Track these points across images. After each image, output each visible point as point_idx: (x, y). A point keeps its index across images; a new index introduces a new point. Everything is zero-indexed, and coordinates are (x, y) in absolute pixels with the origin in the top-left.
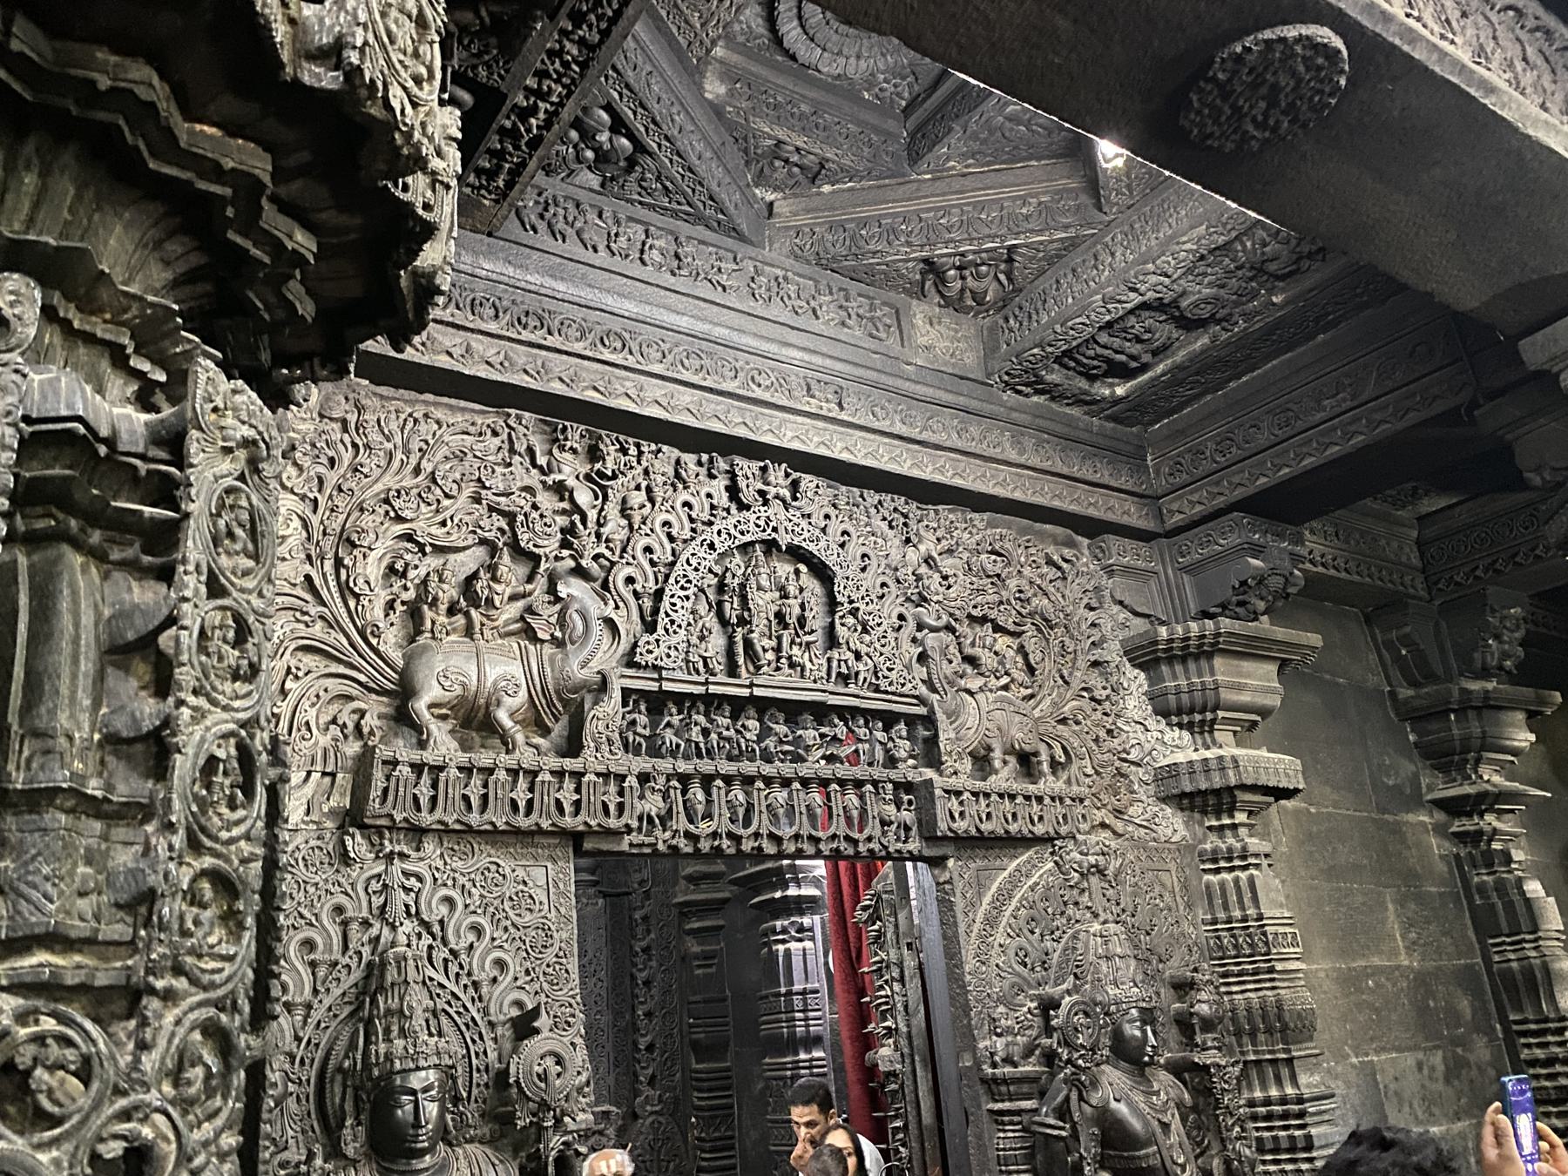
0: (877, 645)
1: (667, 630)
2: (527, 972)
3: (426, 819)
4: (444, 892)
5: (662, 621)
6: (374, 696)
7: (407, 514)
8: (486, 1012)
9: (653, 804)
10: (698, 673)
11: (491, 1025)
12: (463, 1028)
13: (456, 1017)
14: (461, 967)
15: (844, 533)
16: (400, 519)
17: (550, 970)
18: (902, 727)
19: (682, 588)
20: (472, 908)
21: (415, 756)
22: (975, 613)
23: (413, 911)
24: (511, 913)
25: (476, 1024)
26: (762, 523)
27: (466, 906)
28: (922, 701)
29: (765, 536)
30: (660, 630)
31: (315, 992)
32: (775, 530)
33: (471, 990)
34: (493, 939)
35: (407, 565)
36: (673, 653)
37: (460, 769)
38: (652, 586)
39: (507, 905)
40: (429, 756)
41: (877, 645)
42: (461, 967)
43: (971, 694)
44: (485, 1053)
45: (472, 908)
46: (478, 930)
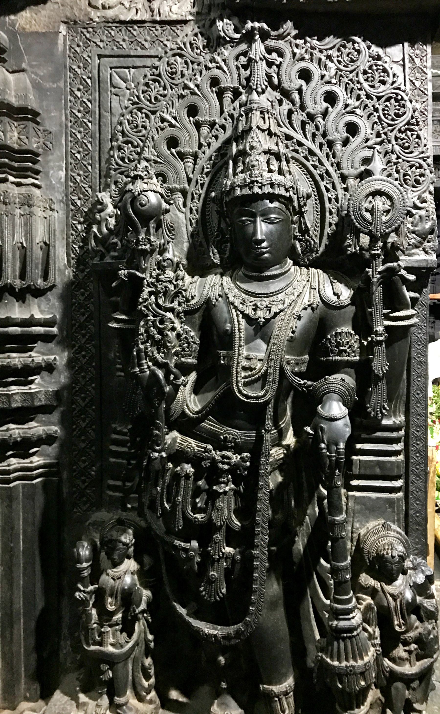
2: (378, 135)
4: (303, 64)
8: (339, 166)
12: (318, 178)
13: (312, 169)
14: (317, 128)
17: (403, 136)
20: (327, 78)
24: (366, 85)
27: (323, 77)
31: (200, 146)
33: (325, 148)
34: (347, 106)
39: (361, 78)
46: (331, 98)
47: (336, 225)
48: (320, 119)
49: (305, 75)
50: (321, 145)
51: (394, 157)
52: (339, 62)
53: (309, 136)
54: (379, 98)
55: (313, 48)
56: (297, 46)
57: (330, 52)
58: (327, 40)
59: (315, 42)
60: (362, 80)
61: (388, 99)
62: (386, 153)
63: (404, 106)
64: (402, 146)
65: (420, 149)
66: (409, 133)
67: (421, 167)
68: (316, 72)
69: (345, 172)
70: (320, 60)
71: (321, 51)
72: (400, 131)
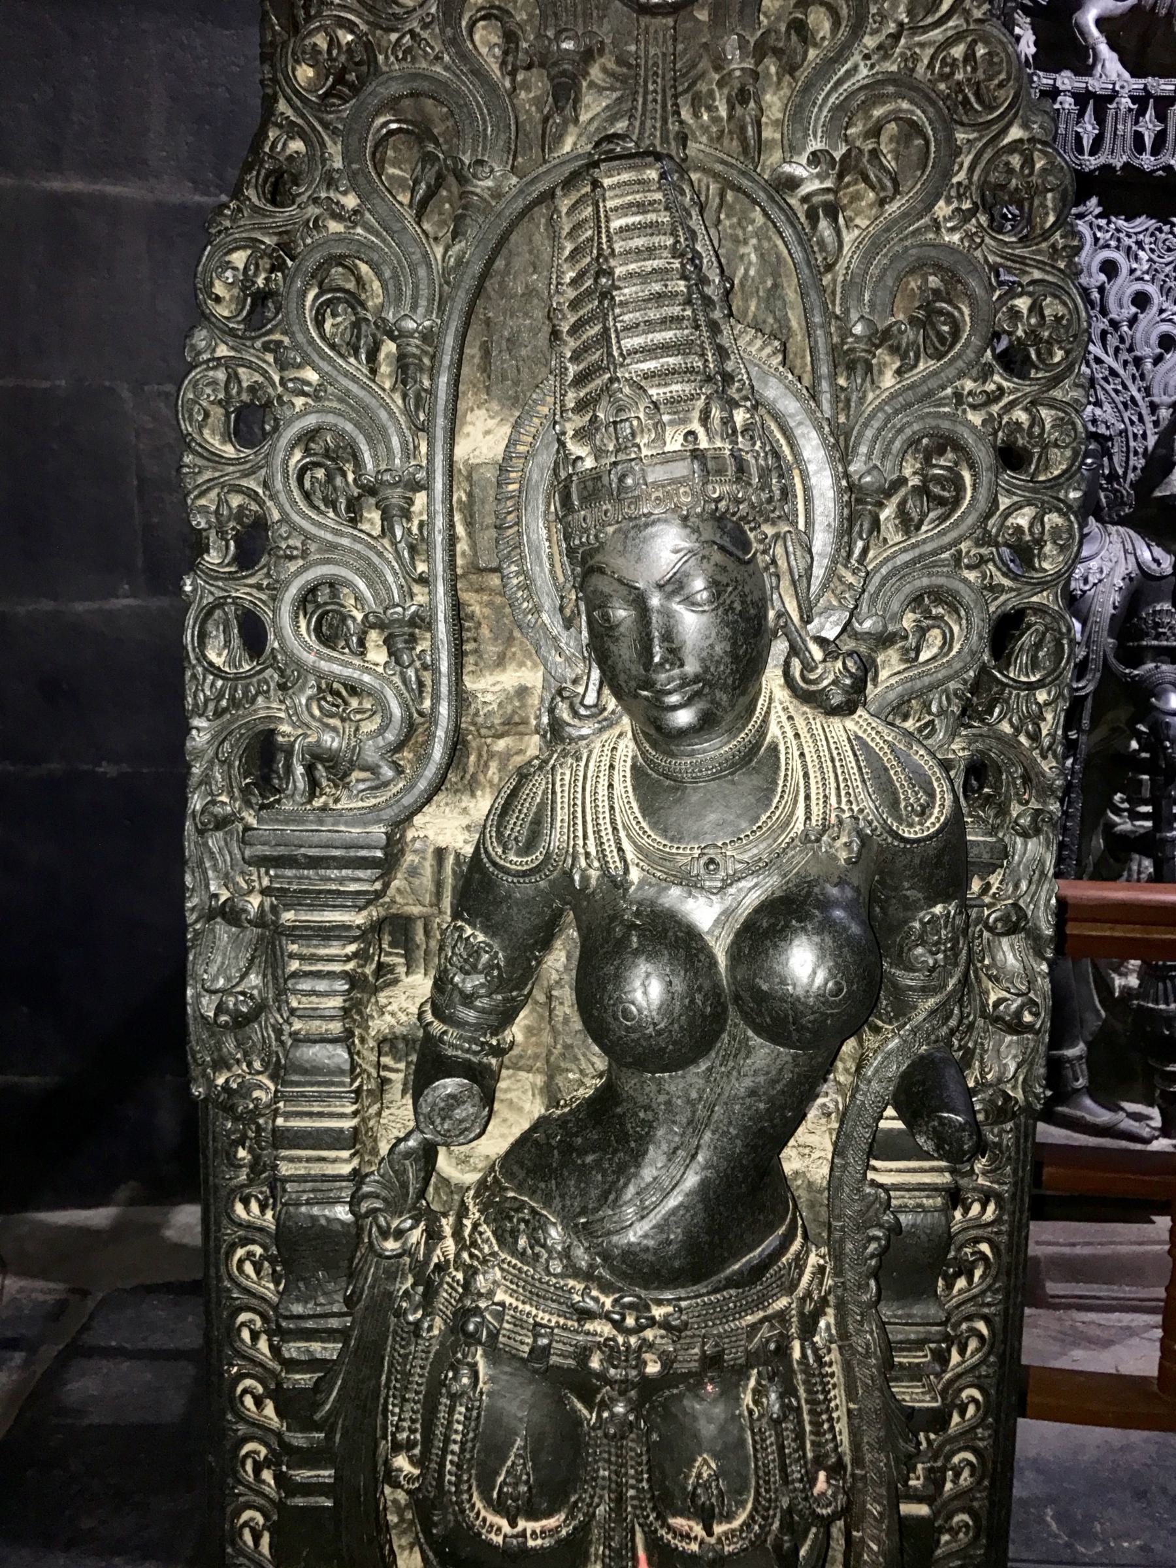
4: (1106, 254)
8: (1148, 391)
11: (1154, 407)
14: (1122, 340)
20: (1138, 273)
21: (1079, 83)
27: (1132, 271)
33: (1132, 369)
37: (1134, 99)
40: (1095, 84)
42: (1122, 340)
44: (1144, 436)
45: (1138, 273)
46: (1141, 300)
47: (1142, 469)
48: (1125, 329)
49: (1110, 268)
50: (1126, 363)
52: (1152, 251)
53: (1111, 351)
55: (1118, 230)
56: (1100, 228)
57: (1141, 237)
58: (1138, 221)
59: (1121, 223)
68: (1124, 264)
69: (1156, 399)
70: (1130, 248)
71: (1129, 236)
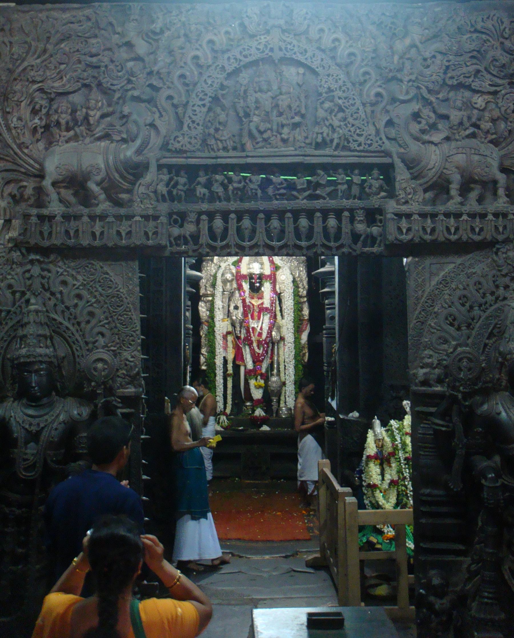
0: (350, 120)
1: (189, 127)
3: (46, 243)
5: (187, 121)
6: (32, 179)
7: (39, 79)
9: (190, 228)
10: (213, 149)
14: (71, 314)
15: (336, 40)
16: (34, 82)
18: (375, 172)
19: (201, 99)
22: (450, 82)
23: (46, 286)
24: (100, 289)
25: (78, 342)
26: (261, 47)
28: (388, 154)
29: (264, 55)
30: (185, 128)
32: (272, 50)
33: (76, 326)
35: (41, 106)
36: (193, 141)
38: (184, 99)
41: (350, 120)
43: (436, 145)
46: (79, 297)
49: (64, 283)
51: (116, 331)
53: (67, 319)
54: (108, 296)
60: (98, 286)
61: (113, 297)
62: (111, 329)
63: (122, 301)
64: (121, 324)
65: (132, 326)
66: (125, 316)
67: (132, 336)
72: (120, 315)
